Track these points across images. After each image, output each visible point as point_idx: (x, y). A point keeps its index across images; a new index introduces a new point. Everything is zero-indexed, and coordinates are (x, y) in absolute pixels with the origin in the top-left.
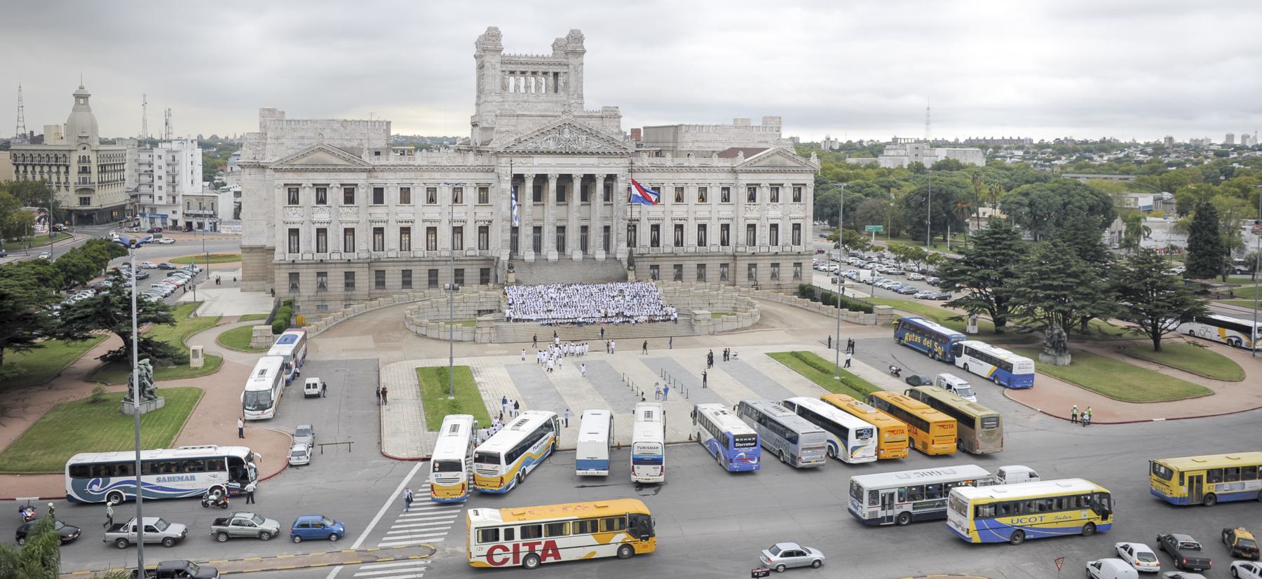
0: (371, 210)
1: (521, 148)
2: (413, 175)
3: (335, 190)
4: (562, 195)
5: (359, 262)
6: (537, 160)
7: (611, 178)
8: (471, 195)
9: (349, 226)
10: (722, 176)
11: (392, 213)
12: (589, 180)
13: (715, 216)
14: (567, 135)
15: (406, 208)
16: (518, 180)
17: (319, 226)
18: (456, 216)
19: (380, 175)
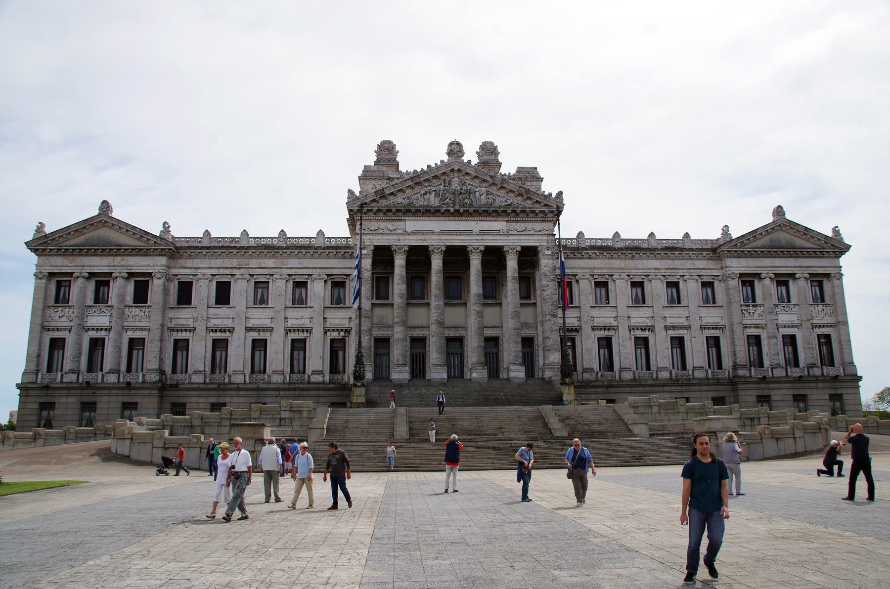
0: (172, 314)
1: (384, 203)
2: (235, 262)
3: (120, 281)
4: (454, 290)
5: (145, 386)
6: (412, 224)
7: (529, 257)
8: (318, 291)
9: (138, 335)
10: (701, 264)
11: (201, 318)
12: (494, 257)
13: (696, 325)
14: (455, 184)
15: (223, 311)
16: (383, 257)
17: (93, 334)
18: (291, 323)
19: (189, 263)
